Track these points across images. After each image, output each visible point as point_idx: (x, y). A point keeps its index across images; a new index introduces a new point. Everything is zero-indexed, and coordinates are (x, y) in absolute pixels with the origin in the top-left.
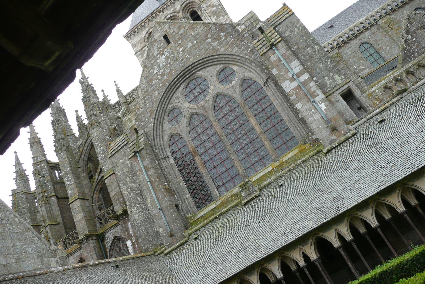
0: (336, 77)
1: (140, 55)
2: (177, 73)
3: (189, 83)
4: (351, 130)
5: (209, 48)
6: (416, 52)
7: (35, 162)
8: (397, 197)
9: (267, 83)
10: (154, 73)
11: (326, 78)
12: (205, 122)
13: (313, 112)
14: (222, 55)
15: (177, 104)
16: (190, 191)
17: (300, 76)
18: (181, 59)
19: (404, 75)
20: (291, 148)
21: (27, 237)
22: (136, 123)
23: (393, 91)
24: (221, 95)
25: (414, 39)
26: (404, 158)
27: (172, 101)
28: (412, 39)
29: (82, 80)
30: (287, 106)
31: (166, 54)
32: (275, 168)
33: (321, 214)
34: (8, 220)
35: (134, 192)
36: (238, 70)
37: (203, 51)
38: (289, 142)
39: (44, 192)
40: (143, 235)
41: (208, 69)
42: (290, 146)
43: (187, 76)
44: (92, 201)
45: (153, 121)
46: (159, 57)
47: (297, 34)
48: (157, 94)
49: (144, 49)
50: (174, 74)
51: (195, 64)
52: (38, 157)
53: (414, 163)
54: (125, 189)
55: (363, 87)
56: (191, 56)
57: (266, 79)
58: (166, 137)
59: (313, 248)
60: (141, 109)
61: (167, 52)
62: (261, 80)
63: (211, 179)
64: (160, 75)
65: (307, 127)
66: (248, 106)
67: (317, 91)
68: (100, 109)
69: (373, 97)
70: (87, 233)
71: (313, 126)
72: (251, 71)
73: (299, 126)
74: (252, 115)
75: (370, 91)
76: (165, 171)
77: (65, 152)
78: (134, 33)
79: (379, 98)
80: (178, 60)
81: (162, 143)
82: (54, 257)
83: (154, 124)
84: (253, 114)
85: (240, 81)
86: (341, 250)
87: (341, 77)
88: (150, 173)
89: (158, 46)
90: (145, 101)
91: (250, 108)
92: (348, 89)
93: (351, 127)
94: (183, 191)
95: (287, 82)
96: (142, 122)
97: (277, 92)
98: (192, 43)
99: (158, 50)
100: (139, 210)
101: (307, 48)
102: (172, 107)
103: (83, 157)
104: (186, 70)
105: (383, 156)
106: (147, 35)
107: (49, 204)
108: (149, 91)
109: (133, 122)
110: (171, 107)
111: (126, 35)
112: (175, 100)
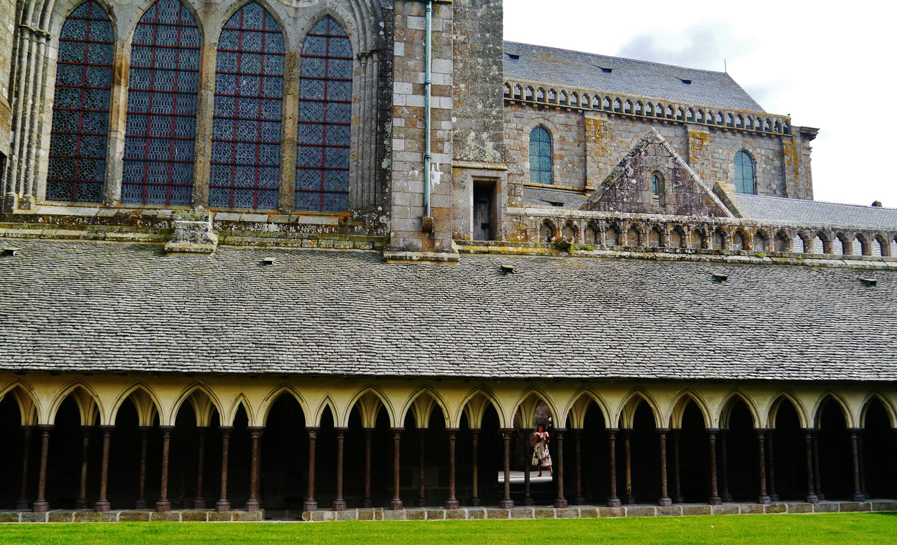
0: (490, 145)
4: (453, 252)
6: (623, 203)
8: (460, 401)
9: (367, 58)
11: (473, 134)
12: (188, 32)
13: (413, 175)
17: (436, 96)
19: (584, 224)
20: (327, 209)
23: (552, 237)
24: (262, 7)
25: (634, 181)
26: (510, 349)
28: (633, 178)
30: (374, 128)
33: (320, 356)
38: (332, 196)
42: (327, 205)
47: (482, 17)
53: (521, 366)
55: (515, 196)
57: (370, 49)
59: (268, 403)
62: (362, 43)
63: (122, 156)
65: (383, 193)
66: (301, 72)
67: (446, 144)
69: (519, 223)
71: (398, 199)
72: (352, 10)
73: (370, 181)
74: (296, 94)
75: (521, 211)
79: (525, 231)
84: (300, 94)
85: (318, 10)
86: (312, 435)
87: (496, 151)
91: (301, 78)
92: (492, 180)
93: (456, 247)
95: (408, 87)
97: (375, 90)
101: (479, 56)
105: (481, 325)
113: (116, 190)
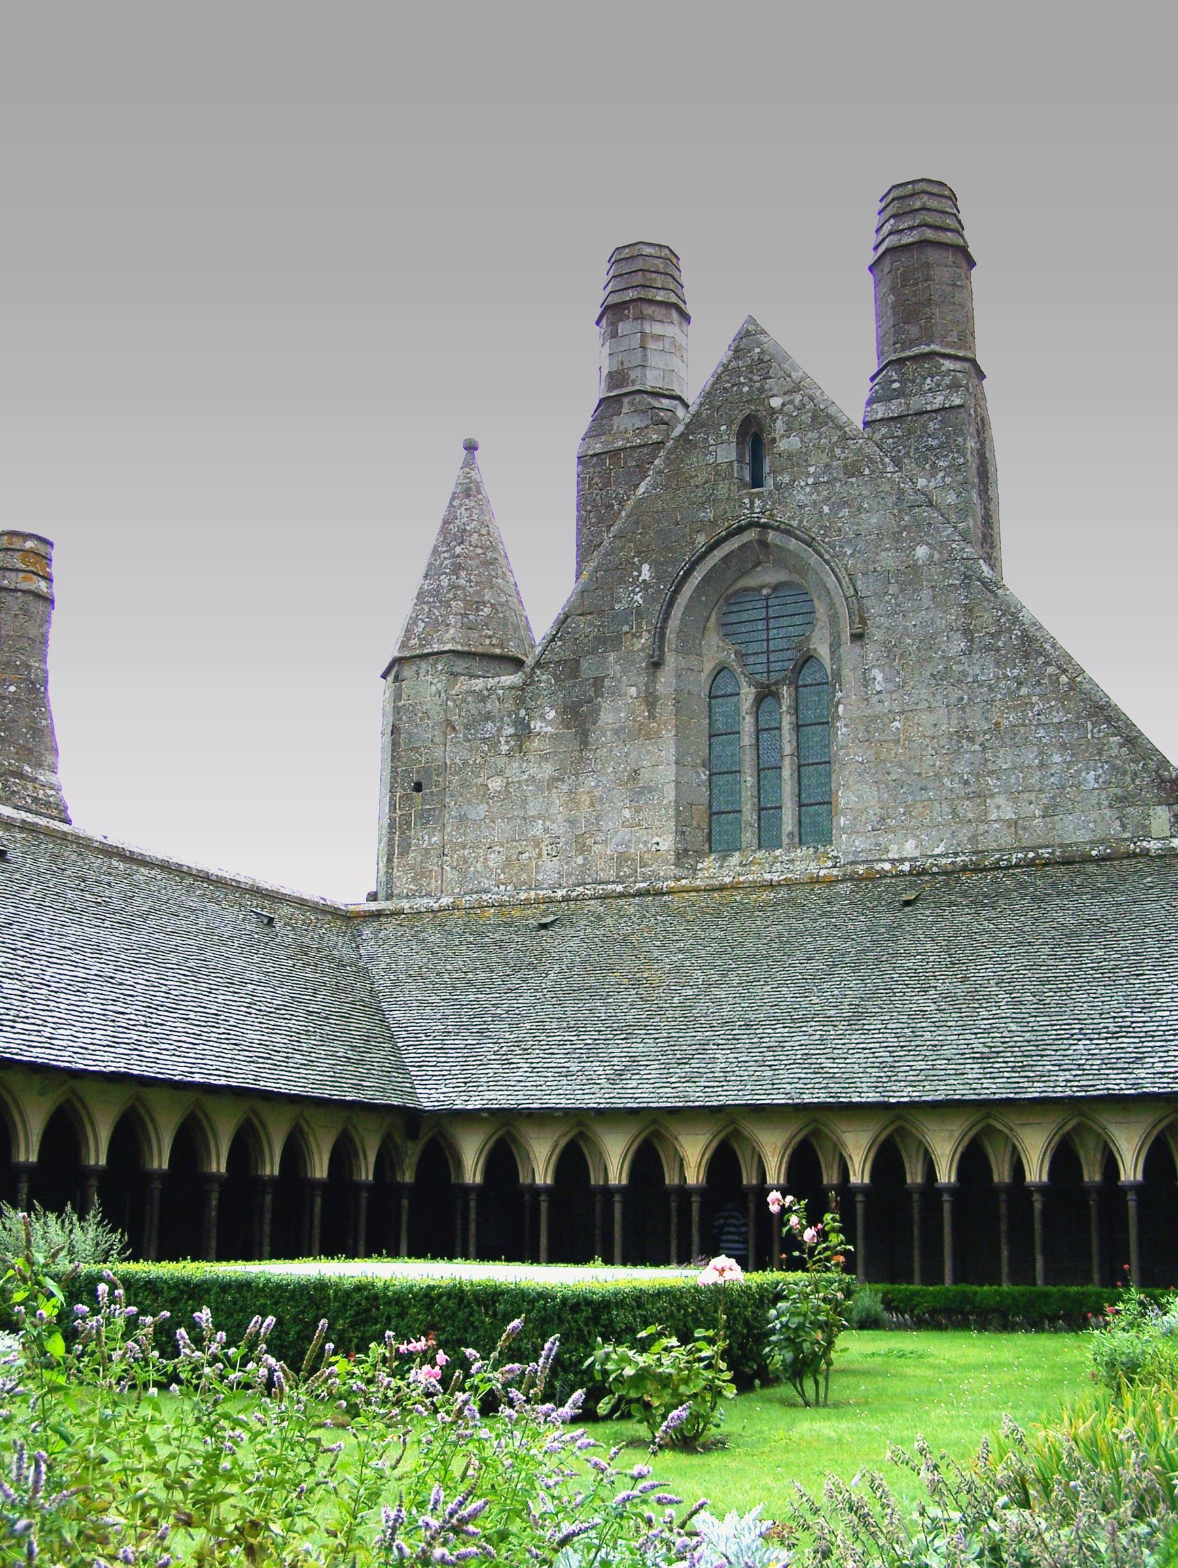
21: (1089, 736)
82: (1169, 805)
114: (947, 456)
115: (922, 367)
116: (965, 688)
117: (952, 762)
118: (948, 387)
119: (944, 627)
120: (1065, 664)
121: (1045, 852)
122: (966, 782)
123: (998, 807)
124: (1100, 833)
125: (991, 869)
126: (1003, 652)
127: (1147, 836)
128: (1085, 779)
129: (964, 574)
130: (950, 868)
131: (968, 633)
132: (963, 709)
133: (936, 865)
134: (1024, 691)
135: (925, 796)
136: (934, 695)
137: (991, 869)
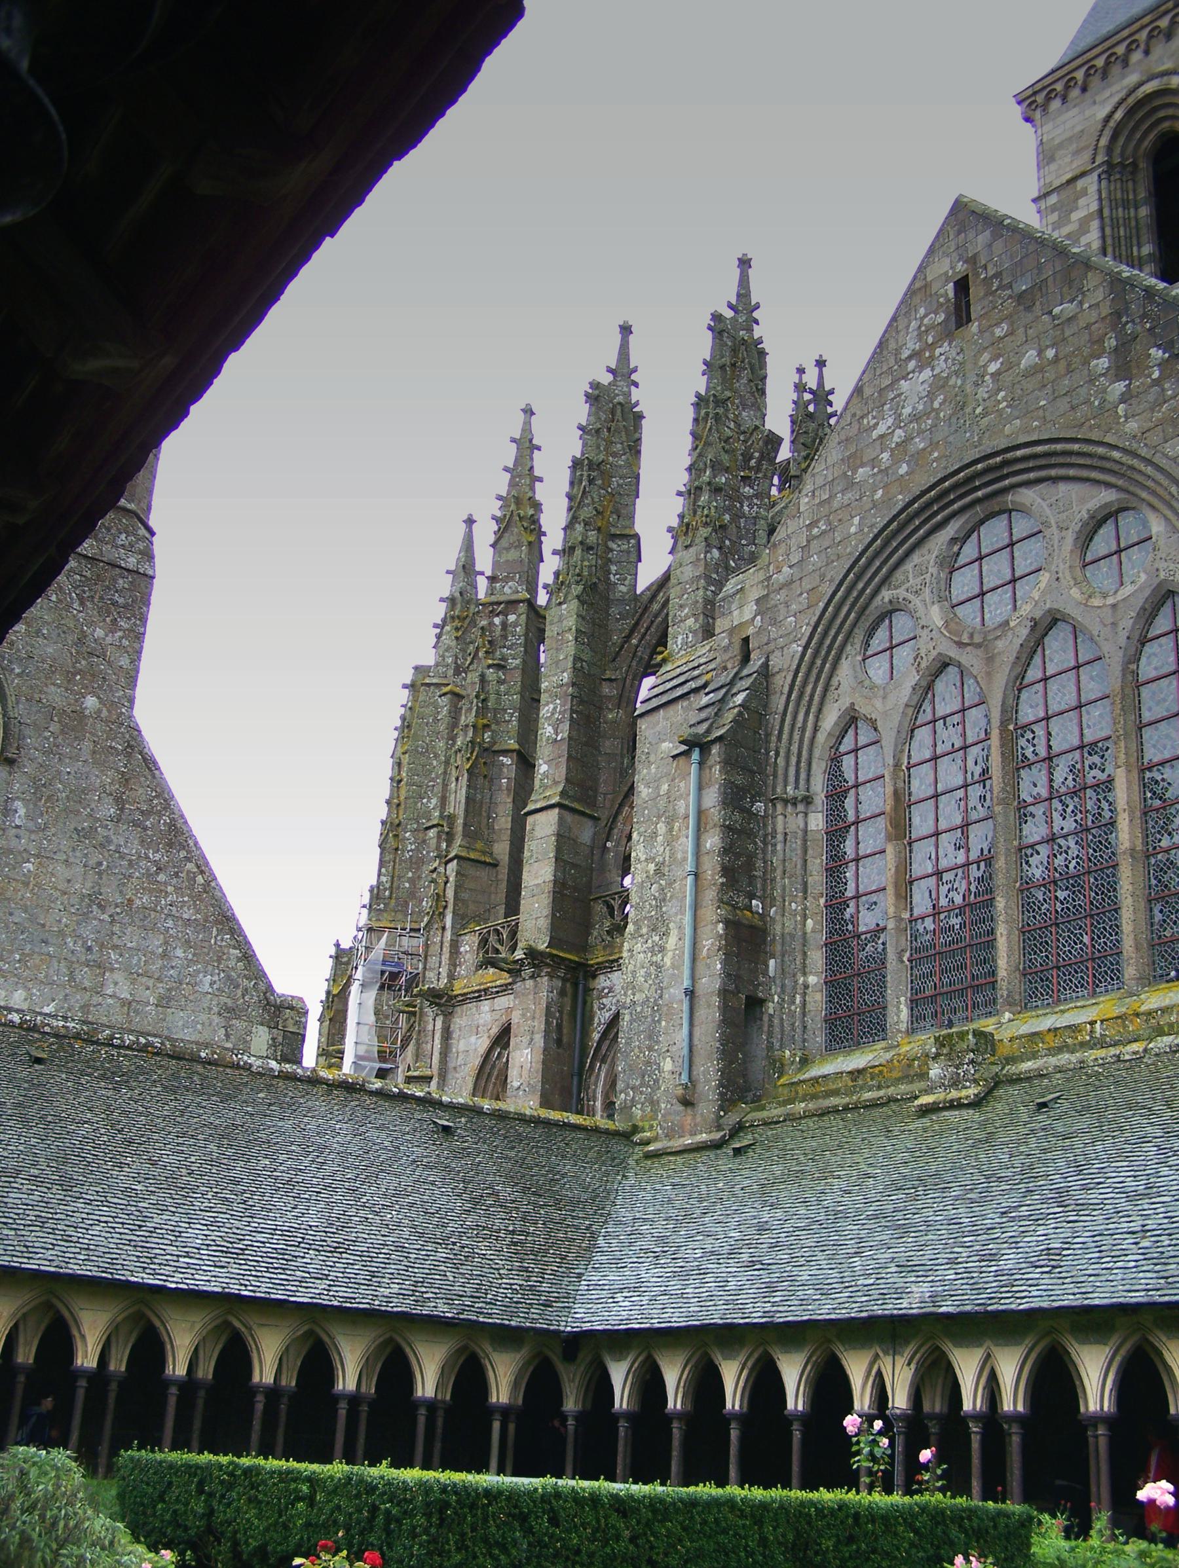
1: (1053, 209)
2: (946, 468)
3: (982, 522)
5: (1087, 402)
7: (493, 599)
10: (875, 434)
14: (1124, 451)
15: (910, 597)
16: (830, 962)
18: (978, 410)
22: (755, 617)
27: (899, 575)
29: (729, 314)
31: (940, 366)
32: (1102, 1021)
34: (176, 875)
35: (663, 882)
36: (1161, 543)
37: (1063, 405)
39: (486, 727)
40: (636, 1050)
41: (1062, 487)
43: (980, 494)
44: (611, 829)
45: (808, 634)
46: (913, 372)
48: (853, 530)
49: (1080, 184)
50: (936, 467)
51: (1019, 453)
52: (506, 580)
54: (643, 858)
56: (1016, 413)
58: (831, 718)
60: (786, 569)
61: (946, 360)
63: (907, 954)
64: (892, 450)
68: (753, 463)
70: (542, 946)
74: (1133, 760)
76: (774, 852)
77: (574, 605)
78: (1067, 87)
80: (968, 410)
81: (808, 734)
82: (270, 1027)
83: (806, 648)
85: (1147, 593)
86: (974, 1428)
88: (708, 845)
89: (926, 321)
90: (808, 541)
94: (805, 954)
96: (774, 622)
98: (1040, 353)
99: (920, 336)
100: (654, 959)
102: (890, 602)
103: (634, 641)
104: (979, 466)
106: (1118, 115)
107: (485, 777)
108: (836, 504)
109: (750, 609)
110: (886, 600)
111: (1030, 92)
112: (911, 576)
113: (900, 1013)
114: (129, 618)
115: (120, 520)
116: (106, 854)
117: (78, 924)
118: (141, 552)
119: (97, 785)
120: (203, 866)
121: (157, 1041)
122: (89, 949)
123: (116, 984)
124: (206, 1036)
125: (103, 1044)
126: (149, 833)
127: (246, 1051)
128: (201, 981)
129: (128, 742)
130: (63, 1031)
131: (120, 802)
132: (100, 874)
133: (48, 1025)
134: (162, 877)
135: (45, 950)
136: (74, 850)
137: (103, 1044)
